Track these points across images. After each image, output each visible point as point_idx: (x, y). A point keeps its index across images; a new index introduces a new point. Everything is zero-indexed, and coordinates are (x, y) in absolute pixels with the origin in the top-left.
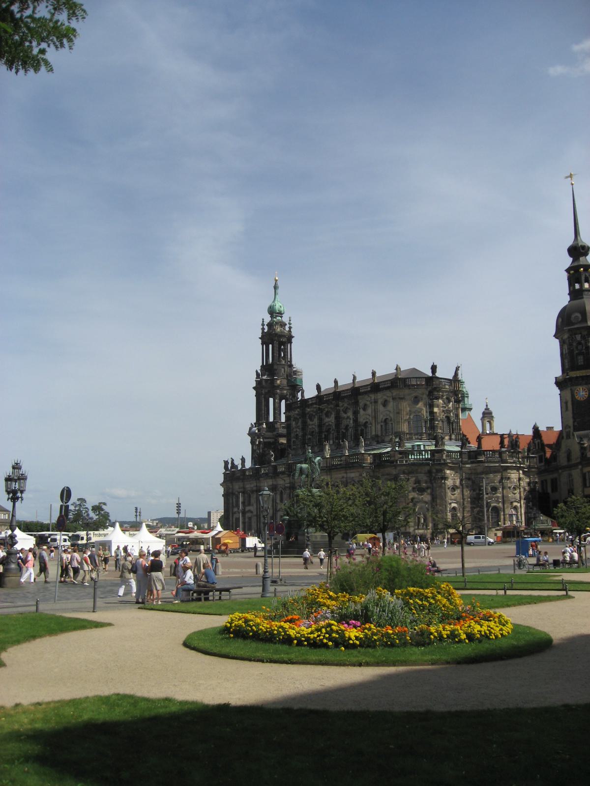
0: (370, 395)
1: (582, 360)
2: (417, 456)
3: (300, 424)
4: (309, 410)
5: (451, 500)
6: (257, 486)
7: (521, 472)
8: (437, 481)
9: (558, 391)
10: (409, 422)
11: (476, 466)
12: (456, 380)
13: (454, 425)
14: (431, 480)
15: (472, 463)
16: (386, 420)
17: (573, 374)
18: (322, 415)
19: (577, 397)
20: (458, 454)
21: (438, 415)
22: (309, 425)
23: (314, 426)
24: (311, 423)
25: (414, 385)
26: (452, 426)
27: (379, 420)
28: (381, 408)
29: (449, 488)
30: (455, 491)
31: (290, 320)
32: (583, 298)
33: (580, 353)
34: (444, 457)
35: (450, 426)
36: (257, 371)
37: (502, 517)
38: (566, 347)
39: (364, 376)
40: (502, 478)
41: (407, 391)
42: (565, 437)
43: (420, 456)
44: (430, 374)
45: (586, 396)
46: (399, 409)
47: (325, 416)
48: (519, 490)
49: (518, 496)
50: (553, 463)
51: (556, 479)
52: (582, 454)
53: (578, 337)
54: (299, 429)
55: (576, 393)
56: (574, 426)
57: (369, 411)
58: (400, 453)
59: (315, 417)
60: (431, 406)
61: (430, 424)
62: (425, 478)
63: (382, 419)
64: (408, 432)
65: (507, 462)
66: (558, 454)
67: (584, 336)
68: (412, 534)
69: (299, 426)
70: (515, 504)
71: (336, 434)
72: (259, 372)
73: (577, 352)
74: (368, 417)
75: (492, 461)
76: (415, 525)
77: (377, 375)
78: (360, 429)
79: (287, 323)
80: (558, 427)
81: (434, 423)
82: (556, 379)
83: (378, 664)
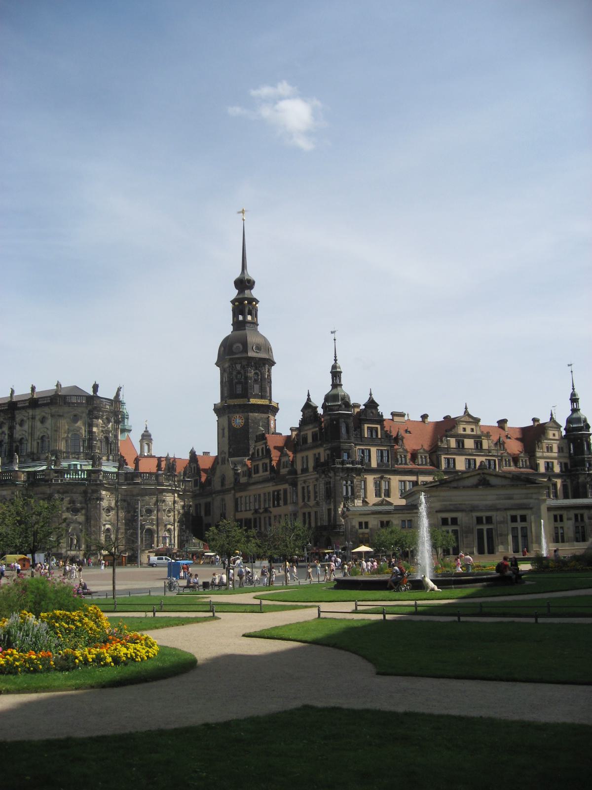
0: (28, 411)
1: (240, 389)
2: (73, 475)
5: (105, 521)
7: (176, 495)
8: (92, 502)
9: (216, 418)
10: (66, 441)
11: (131, 488)
12: (117, 401)
13: (113, 445)
14: (86, 501)
15: (129, 484)
16: (42, 438)
19: (233, 424)
20: (115, 475)
21: (97, 435)
25: (73, 403)
26: (111, 447)
28: (38, 424)
29: (104, 509)
30: (110, 512)
32: (245, 329)
33: (239, 382)
34: (101, 478)
35: (108, 447)
37: (156, 539)
38: (226, 375)
39: (22, 391)
40: (157, 501)
41: (66, 409)
42: (220, 463)
43: (76, 475)
44: (92, 394)
45: (242, 423)
46: (57, 427)
48: (173, 513)
49: (172, 518)
50: (208, 488)
51: (210, 503)
52: (236, 479)
53: (238, 367)
55: (233, 420)
56: (229, 453)
57: (26, 427)
58: (56, 471)
60: (91, 425)
61: (88, 443)
62: (80, 498)
63: (39, 436)
64: (65, 450)
65: (163, 485)
66: (212, 479)
68: (64, 555)
70: (169, 526)
73: (236, 381)
74: (24, 433)
75: (148, 483)
76: (67, 546)
77: (37, 390)
78: (15, 445)
80: (214, 453)
81: (92, 443)
83: (19, 691)
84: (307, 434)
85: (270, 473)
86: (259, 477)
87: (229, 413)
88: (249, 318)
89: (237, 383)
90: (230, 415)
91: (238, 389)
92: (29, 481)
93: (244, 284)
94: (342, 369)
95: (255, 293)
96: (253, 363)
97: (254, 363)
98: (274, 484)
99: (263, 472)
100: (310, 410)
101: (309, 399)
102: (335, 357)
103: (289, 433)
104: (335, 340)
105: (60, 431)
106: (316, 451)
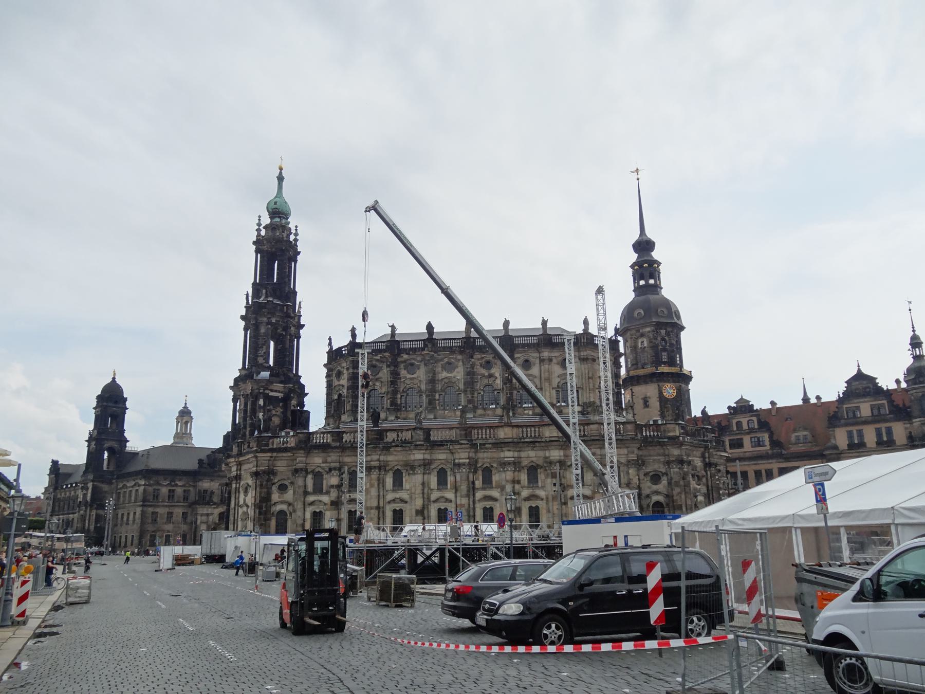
4: (405, 356)
6: (379, 460)
19: (665, 394)
22: (406, 377)
23: (416, 381)
24: (409, 376)
27: (555, 384)
28: (557, 370)
31: (296, 230)
33: (664, 350)
47: (440, 369)
53: (663, 332)
54: (382, 382)
59: (419, 369)
63: (559, 383)
69: (381, 378)
71: (470, 396)
73: (661, 347)
77: (549, 325)
79: (293, 231)
84: (859, 407)
85: (771, 448)
87: (658, 381)
90: (661, 384)
93: (644, 246)
94: (922, 339)
95: (656, 255)
98: (783, 460)
99: (752, 447)
100: (865, 382)
101: (859, 370)
102: (913, 328)
103: (770, 407)
104: (910, 310)
106: (883, 426)
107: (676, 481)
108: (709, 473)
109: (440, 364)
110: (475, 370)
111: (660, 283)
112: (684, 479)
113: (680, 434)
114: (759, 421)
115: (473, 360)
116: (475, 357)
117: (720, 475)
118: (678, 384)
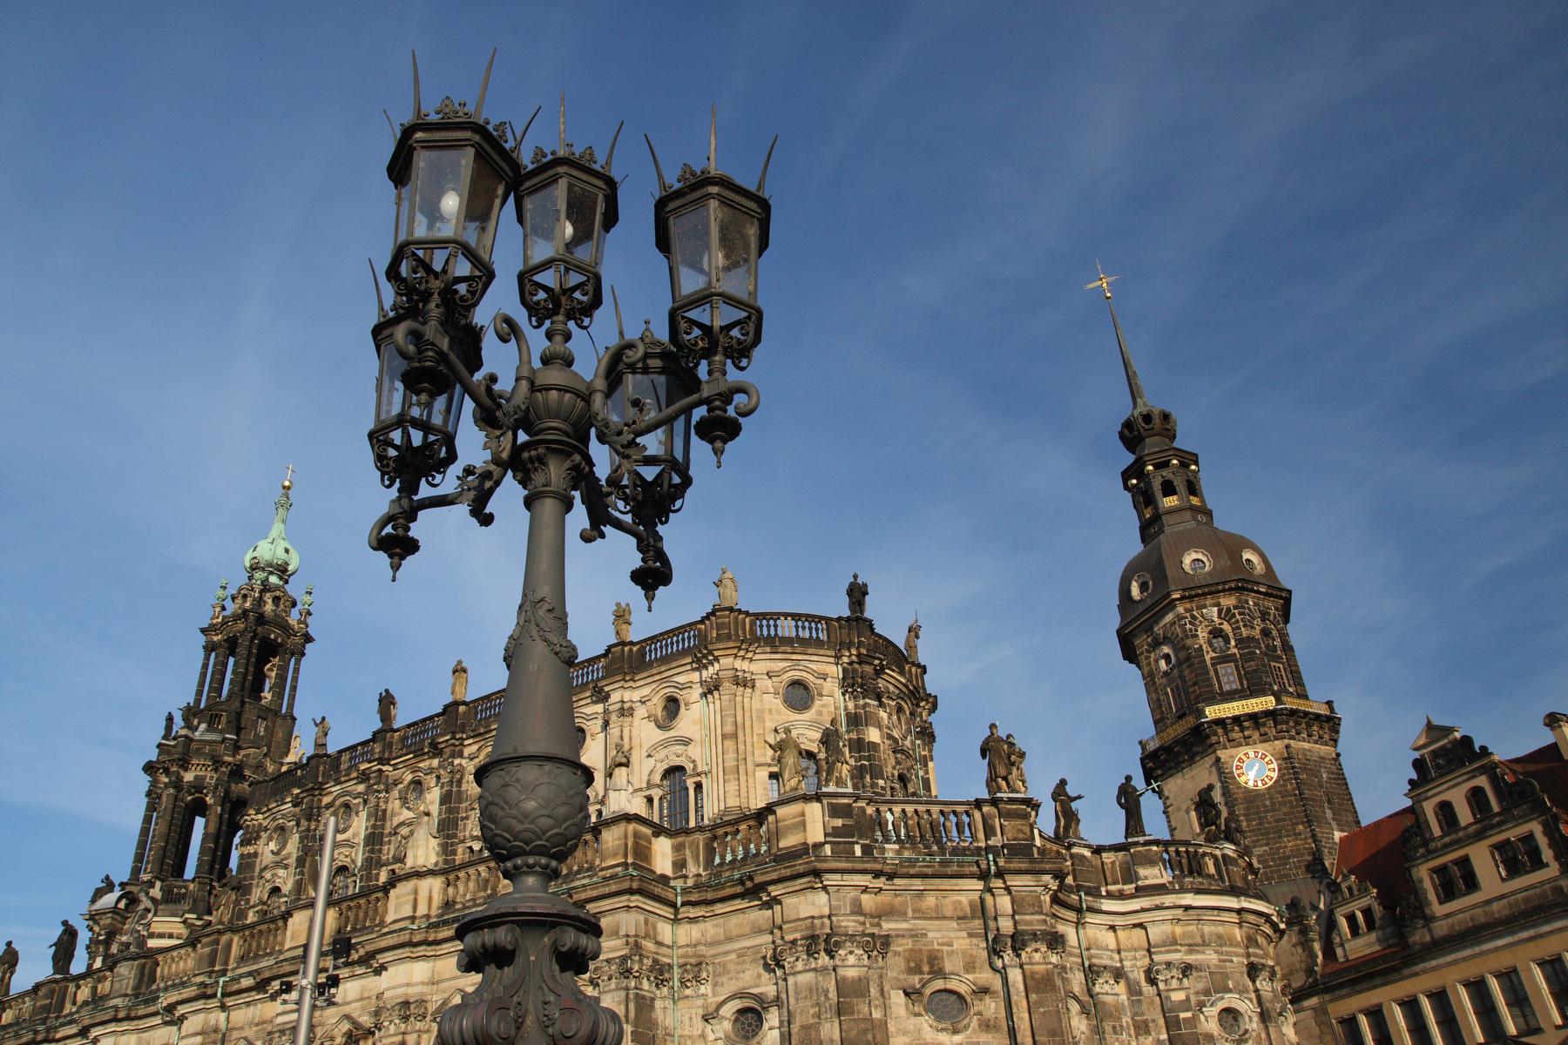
1: (1234, 677)
3: (293, 847)
11: (1143, 910)
14: (995, 951)
15: (1121, 896)
17: (1213, 712)
18: (386, 802)
25: (787, 641)
33: (1224, 659)
36: (170, 719)
44: (846, 613)
54: (286, 867)
67: (1228, 610)
69: (288, 856)
72: (179, 721)
82: (1144, 748)
86: (1488, 902)
88: (1195, 501)
89: (1217, 661)
90: (1223, 754)
91: (1225, 679)
92: (685, 877)
96: (1251, 603)
97: (1255, 604)
103: (1545, 738)
105: (749, 740)
107: (803, 1027)
108: (1015, 976)
109: (395, 793)
110: (464, 788)
111: (1202, 500)
112: (840, 1011)
113: (826, 835)
114: (1496, 781)
115: (457, 761)
116: (467, 751)
117: (1200, 986)
118: (1279, 744)
